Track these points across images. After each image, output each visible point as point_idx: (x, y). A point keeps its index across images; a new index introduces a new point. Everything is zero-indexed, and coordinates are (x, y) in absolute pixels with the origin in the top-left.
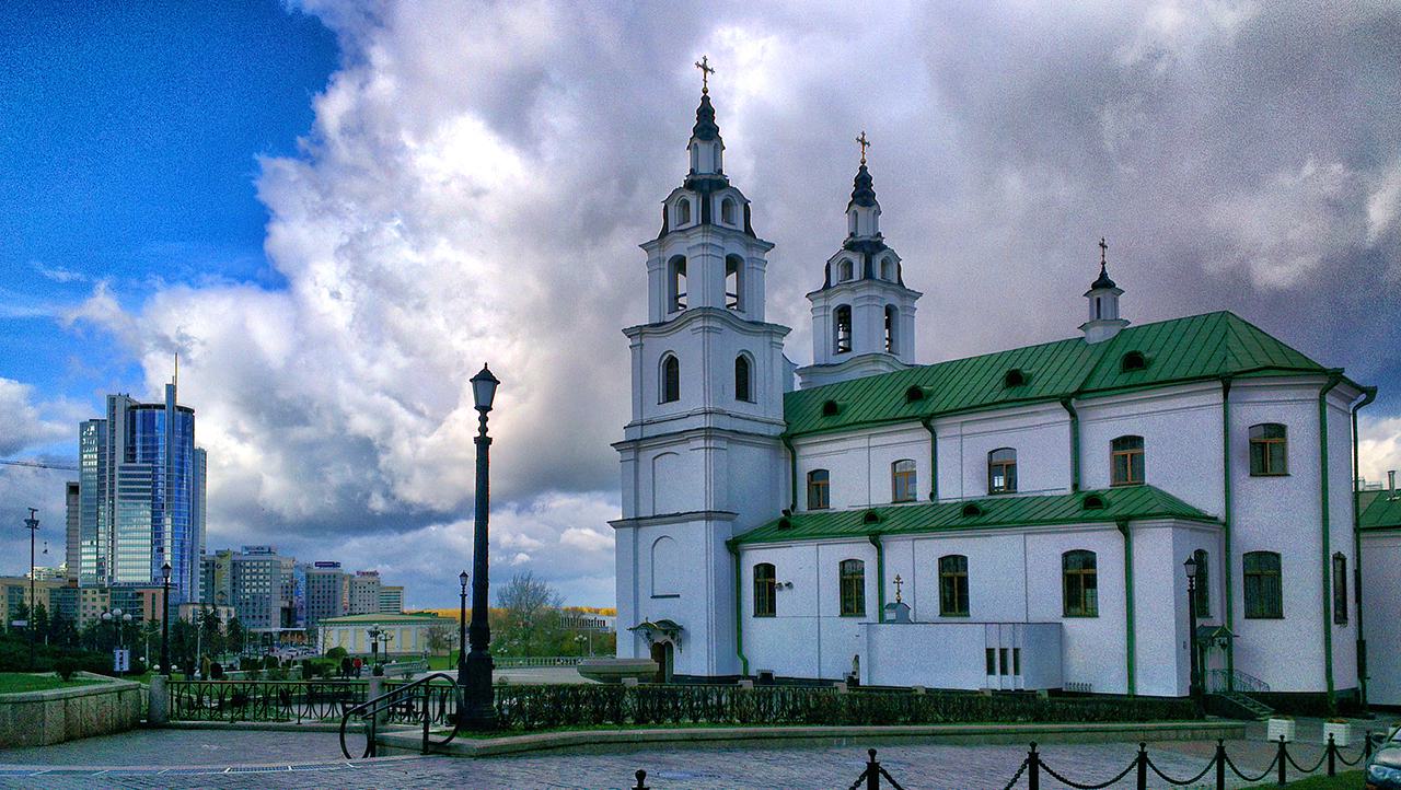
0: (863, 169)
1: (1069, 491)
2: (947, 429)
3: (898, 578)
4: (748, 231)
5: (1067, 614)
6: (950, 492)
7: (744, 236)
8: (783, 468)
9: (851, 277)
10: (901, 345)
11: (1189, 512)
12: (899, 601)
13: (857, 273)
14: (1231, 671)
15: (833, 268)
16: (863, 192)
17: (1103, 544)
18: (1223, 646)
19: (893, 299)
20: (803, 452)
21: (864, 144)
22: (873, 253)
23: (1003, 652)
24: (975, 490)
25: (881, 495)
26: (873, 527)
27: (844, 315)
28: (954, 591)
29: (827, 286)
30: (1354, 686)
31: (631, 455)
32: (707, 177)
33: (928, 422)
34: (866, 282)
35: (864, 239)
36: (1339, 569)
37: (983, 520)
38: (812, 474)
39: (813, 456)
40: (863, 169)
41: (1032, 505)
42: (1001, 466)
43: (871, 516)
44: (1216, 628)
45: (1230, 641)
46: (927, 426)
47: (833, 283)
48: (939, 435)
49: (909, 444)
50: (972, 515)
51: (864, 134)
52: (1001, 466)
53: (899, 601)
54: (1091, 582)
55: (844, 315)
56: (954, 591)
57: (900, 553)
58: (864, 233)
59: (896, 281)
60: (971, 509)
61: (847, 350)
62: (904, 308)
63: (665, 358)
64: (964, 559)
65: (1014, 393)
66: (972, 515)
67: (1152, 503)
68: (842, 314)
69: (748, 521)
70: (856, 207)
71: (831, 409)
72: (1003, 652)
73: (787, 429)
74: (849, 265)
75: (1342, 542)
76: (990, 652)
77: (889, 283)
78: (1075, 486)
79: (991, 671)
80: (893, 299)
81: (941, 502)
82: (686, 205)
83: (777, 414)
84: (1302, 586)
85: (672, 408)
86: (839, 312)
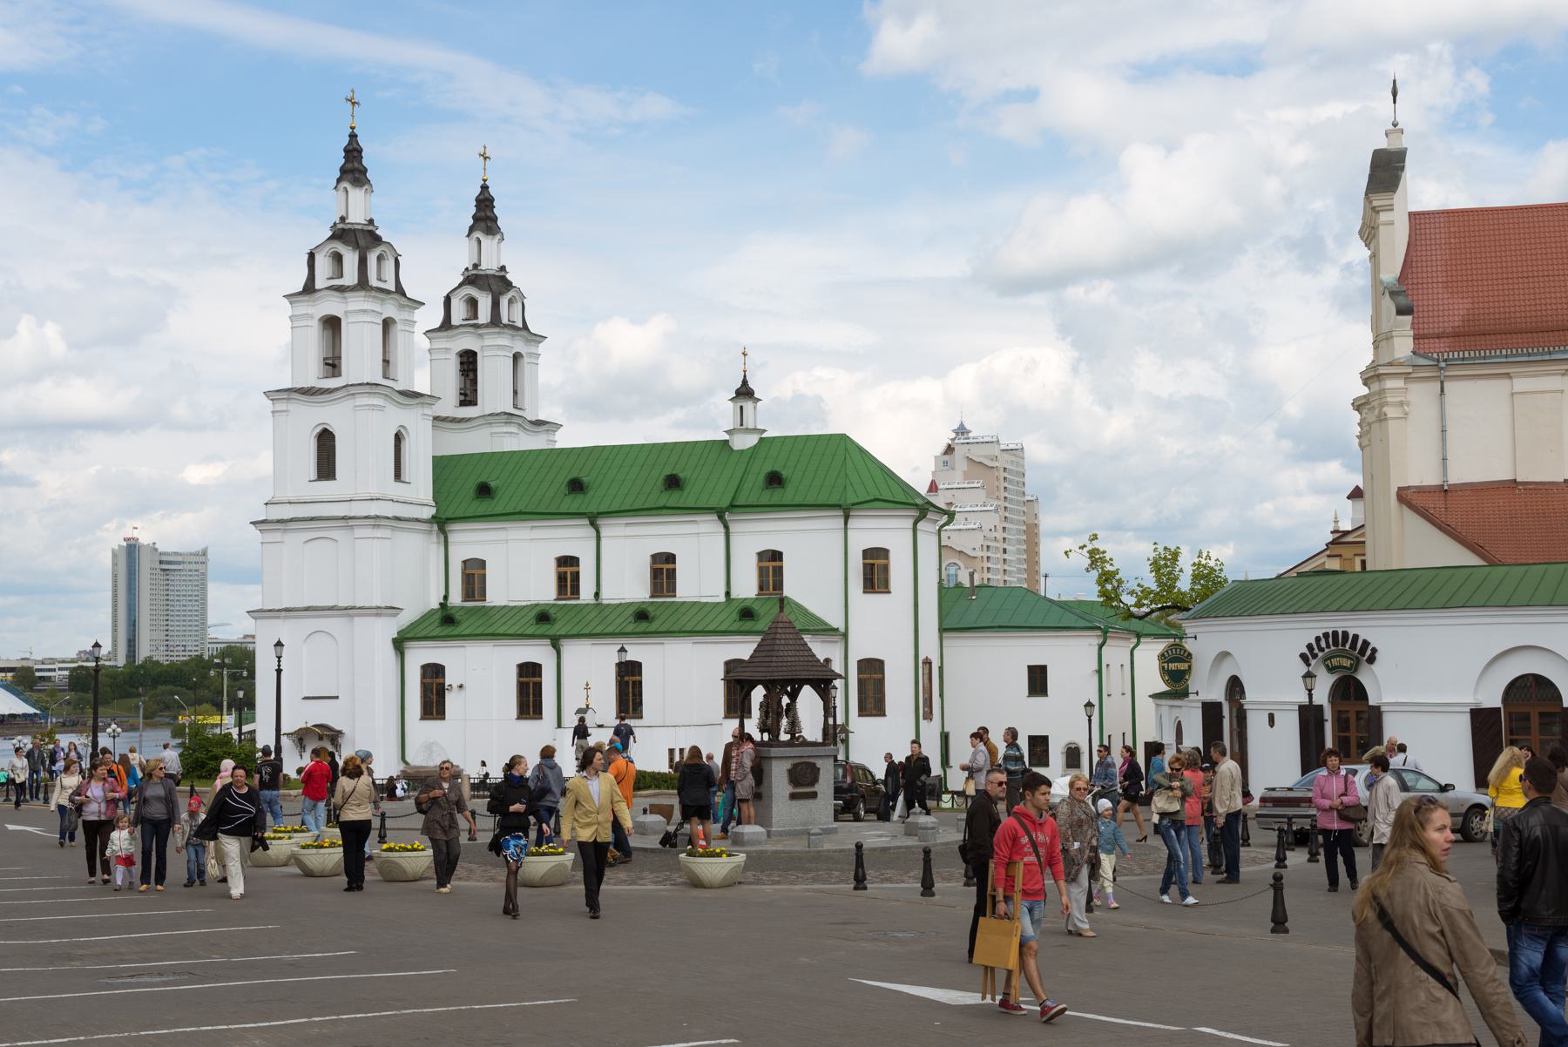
0: (485, 188)
1: (722, 599)
2: (613, 531)
3: (587, 685)
4: (400, 290)
6: (610, 595)
7: (397, 296)
8: (436, 552)
9: (476, 317)
11: (825, 627)
12: (587, 706)
13: (484, 315)
16: (485, 218)
18: (842, 741)
19: (519, 346)
20: (451, 538)
21: (485, 158)
22: (501, 293)
25: (544, 591)
26: (544, 629)
27: (468, 361)
29: (447, 324)
31: (277, 536)
32: (359, 227)
33: (593, 520)
34: (497, 330)
35: (488, 272)
36: (927, 671)
37: (654, 627)
38: (465, 562)
39: (469, 542)
40: (485, 188)
42: (663, 569)
43: (543, 616)
45: (847, 737)
46: (593, 524)
47: (456, 320)
48: (603, 533)
49: (572, 539)
50: (642, 620)
51: (485, 147)
52: (663, 569)
53: (587, 706)
55: (468, 361)
57: (574, 652)
58: (489, 265)
59: (520, 325)
60: (642, 615)
61: (473, 403)
63: (319, 430)
64: (639, 665)
66: (642, 620)
68: (465, 359)
70: (478, 234)
71: (484, 491)
74: (473, 303)
75: (929, 649)
77: (512, 327)
78: (728, 594)
81: (605, 602)
82: (338, 258)
84: (899, 688)
85: (326, 485)
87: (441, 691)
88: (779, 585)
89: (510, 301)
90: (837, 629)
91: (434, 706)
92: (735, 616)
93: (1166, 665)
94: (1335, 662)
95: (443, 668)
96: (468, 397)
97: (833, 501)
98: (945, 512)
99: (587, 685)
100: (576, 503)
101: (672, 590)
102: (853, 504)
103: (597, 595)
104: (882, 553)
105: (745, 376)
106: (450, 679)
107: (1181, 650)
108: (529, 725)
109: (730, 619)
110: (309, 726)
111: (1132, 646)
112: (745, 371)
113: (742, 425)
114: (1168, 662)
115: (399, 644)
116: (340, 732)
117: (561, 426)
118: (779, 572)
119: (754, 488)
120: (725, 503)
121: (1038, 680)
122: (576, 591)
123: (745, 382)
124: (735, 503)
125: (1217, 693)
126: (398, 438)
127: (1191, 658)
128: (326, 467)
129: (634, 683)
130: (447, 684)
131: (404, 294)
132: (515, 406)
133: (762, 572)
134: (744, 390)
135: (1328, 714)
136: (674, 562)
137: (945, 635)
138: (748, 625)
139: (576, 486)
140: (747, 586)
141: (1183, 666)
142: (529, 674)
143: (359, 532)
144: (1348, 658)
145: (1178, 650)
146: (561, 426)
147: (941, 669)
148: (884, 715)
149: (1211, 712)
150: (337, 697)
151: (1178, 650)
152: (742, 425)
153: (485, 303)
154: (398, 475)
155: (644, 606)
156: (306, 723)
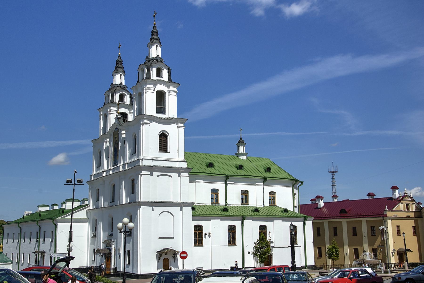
63: (161, 133)
87: (200, 235)
99: (270, 233)
103: (226, 202)
105: (241, 137)
112: (241, 135)
123: (241, 139)
139: (211, 165)
142: (232, 230)
156: (171, 248)
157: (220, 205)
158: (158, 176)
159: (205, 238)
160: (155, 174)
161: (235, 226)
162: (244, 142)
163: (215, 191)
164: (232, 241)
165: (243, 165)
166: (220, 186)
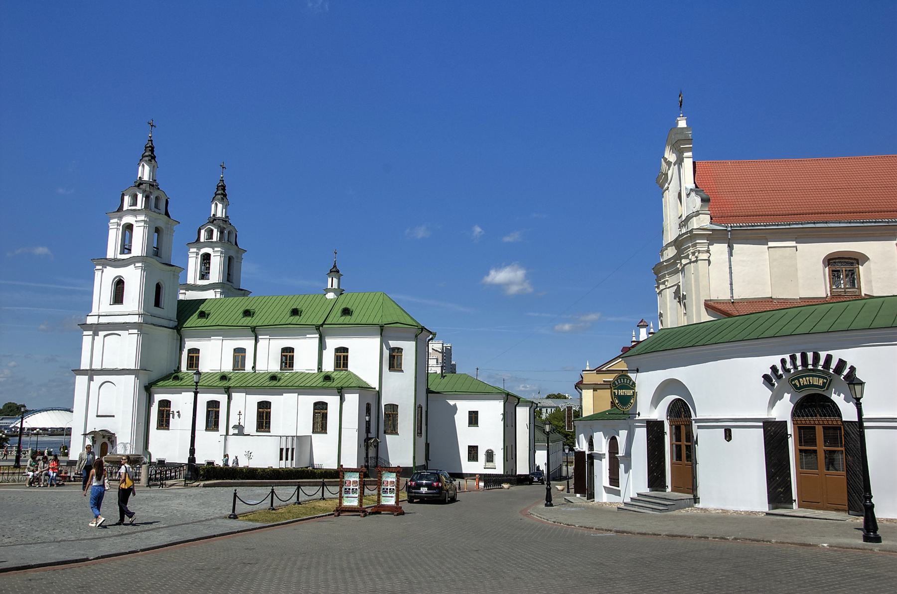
3: (240, 412)
4: (167, 214)
5: (313, 432)
6: (261, 367)
9: (212, 239)
10: (234, 280)
12: (239, 423)
14: (377, 457)
15: (203, 232)
17: (332, 401)
18: (375, 446)
23: (287, 450)
24: (275, 367)
26: (225, 383)
28: (264, 421)
30: (424, 464)
37: (278, 384)
38: (190, 351)
41: (300, 377)
42: (287, 357)
43: (224, 377)
44: (372, 438)
52: (287, 357)
53: (239, 423)
54: (325, 417)
55: (206, 258)
56: (264, 421)
60: (274, 378)
62: (237, 257)
65: (295, 319)
67: (351, 380)
69: (155, 376)
72: (287, 450)
73: (178, 324)
76: (281, 450)
78: (319, 369)
79: (281, 459)
80: (233, 254)
82: (135, 198)
83: (173, 314)
85: (117, 308)
86: (204, 256)
88: (346, 365)
89: (229, 233)
90: (375, 388)
91: (164, 422)
92: (321, 379)
93: (616, 391)
94: (803, 381)
95: (170, 402)
96: (204, 275)
97: (376, 322)
98: (431, 333)
99: (240, 412)
100: (247, 321)
101: (291, 365)
102: (385, 324)
104: (400, 350)
105: (335, 263)
106: (173, 408)
107: (627, 379)
108: (212, 434)
109: (319, 382)
110: (96, 430)
111: (515, 404)
113: (332, 286)
114: (618, 389)
115: (148, 389)
116: (114, 434)
117: (251, 292)
118: (346, 358)
119: (336, 317)
120: (321, 322)
121: (473, 418)
122: (243, 365)
123: (335, 266)
124: (325, 323)
125: (659, 414)
126: (158, 287)
127: (635, 386)
128: (118, 297)
129: (267, 412)
130: (171, 410)
131: (169, 216)
132: (228, 281)
133: (337, 359)
134: (334, 270)
135: (790, 430)
136: (293, 352)
137: (429, 395)
138: (328, 383)
140: (329, 365)
141: (629, 393)
142: (213, 405)
143: (131, 331)
144: (819, 377)
145: (625, 380)
146: (251, 292)
147: (427, 412)
148: (397, 434)
149: (654, 429)
150: (113, 416)
151: (625, 380)
152: (332, 286)
153: (215, 234)
154: (157, 304)
155: (276, 374)
157: (246, 371)
158: (105, 336)
159: (173, 418)
160: (102, 334)
161: (270, 403)
162: (338, 272)
163: (239, 353)
164: (212, 423)
165: (341, 309)
166: (247, 344)
